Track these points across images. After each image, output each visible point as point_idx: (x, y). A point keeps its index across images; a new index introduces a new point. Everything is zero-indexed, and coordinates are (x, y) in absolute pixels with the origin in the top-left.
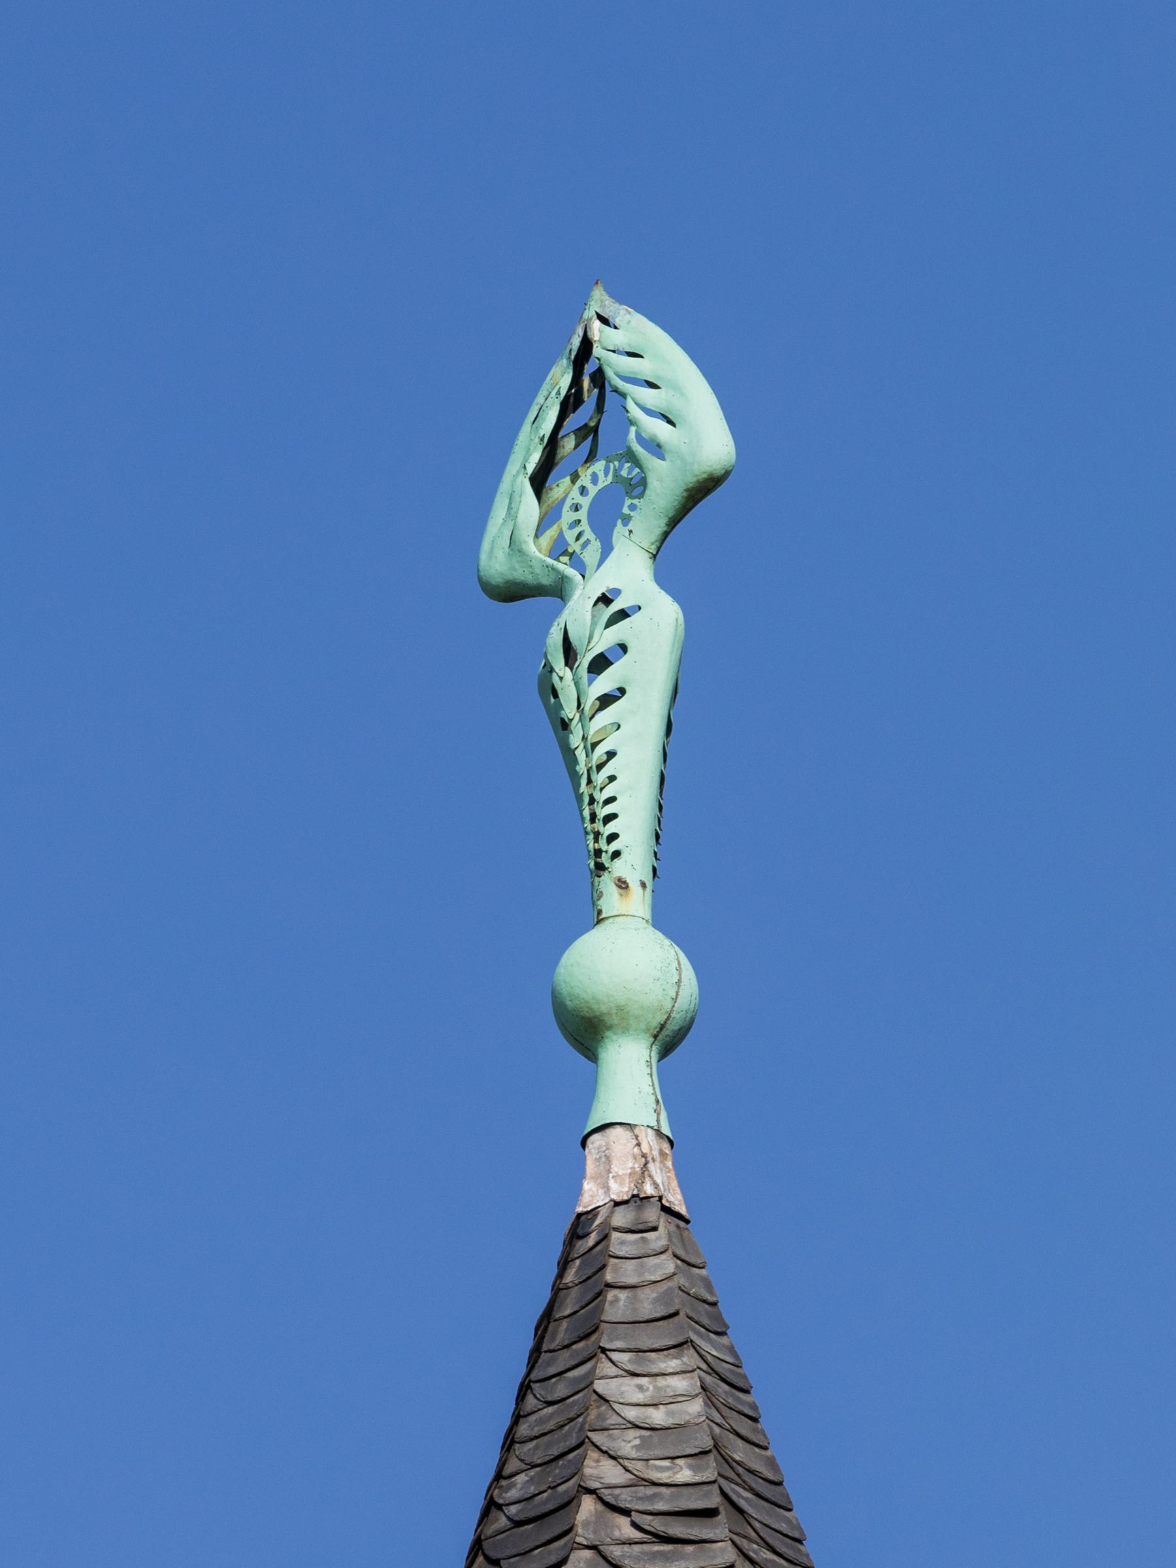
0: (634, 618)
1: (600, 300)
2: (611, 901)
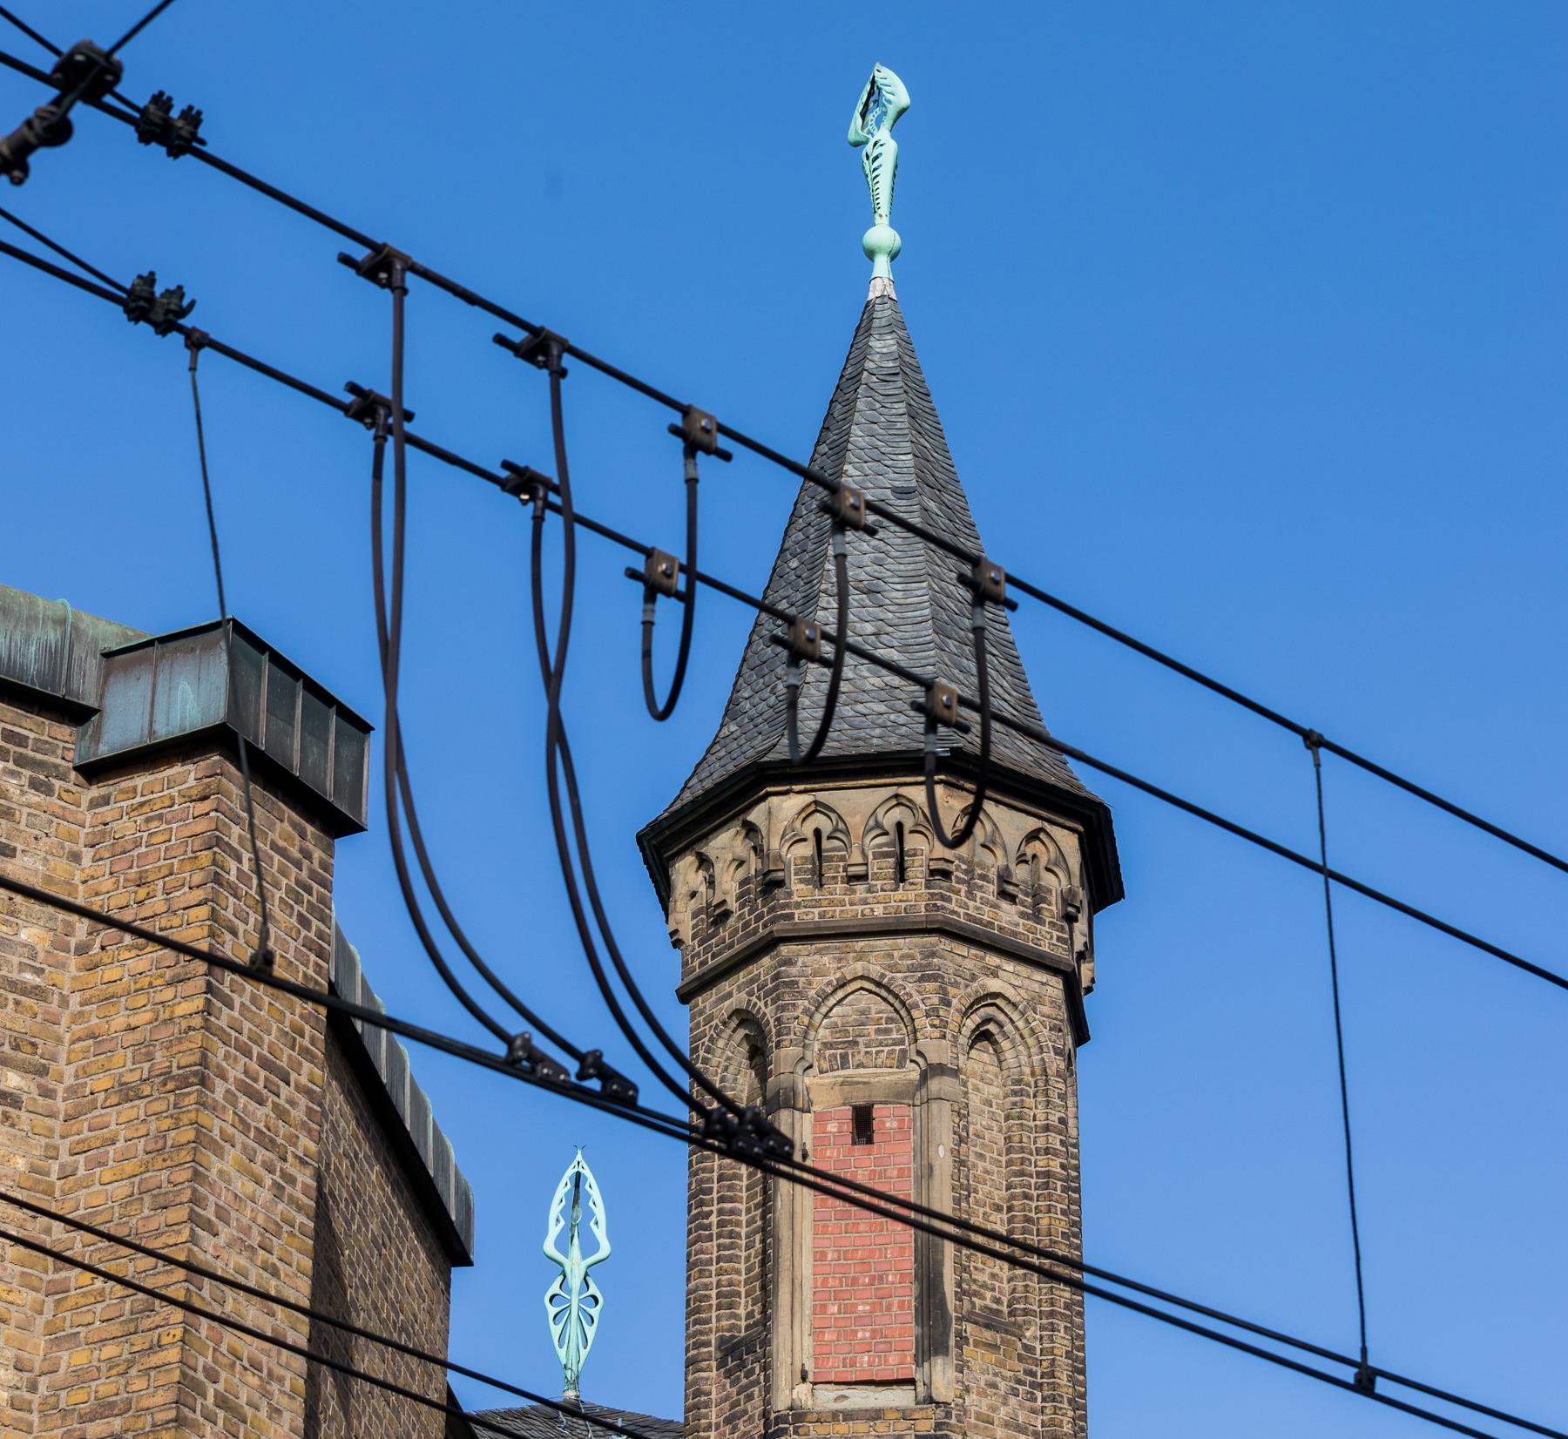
0: (885, 147)
1: (878, 66)
2: (878, 220)
